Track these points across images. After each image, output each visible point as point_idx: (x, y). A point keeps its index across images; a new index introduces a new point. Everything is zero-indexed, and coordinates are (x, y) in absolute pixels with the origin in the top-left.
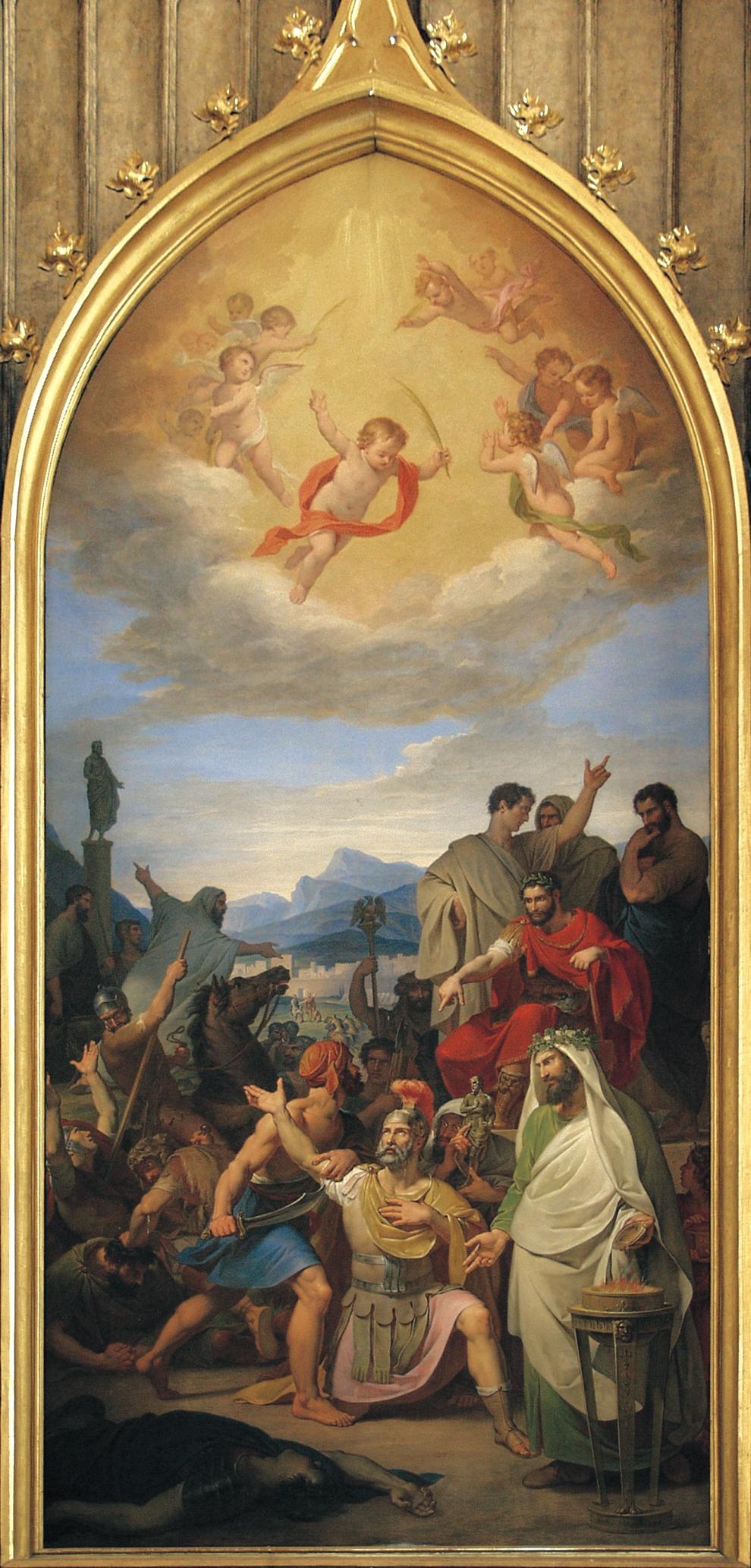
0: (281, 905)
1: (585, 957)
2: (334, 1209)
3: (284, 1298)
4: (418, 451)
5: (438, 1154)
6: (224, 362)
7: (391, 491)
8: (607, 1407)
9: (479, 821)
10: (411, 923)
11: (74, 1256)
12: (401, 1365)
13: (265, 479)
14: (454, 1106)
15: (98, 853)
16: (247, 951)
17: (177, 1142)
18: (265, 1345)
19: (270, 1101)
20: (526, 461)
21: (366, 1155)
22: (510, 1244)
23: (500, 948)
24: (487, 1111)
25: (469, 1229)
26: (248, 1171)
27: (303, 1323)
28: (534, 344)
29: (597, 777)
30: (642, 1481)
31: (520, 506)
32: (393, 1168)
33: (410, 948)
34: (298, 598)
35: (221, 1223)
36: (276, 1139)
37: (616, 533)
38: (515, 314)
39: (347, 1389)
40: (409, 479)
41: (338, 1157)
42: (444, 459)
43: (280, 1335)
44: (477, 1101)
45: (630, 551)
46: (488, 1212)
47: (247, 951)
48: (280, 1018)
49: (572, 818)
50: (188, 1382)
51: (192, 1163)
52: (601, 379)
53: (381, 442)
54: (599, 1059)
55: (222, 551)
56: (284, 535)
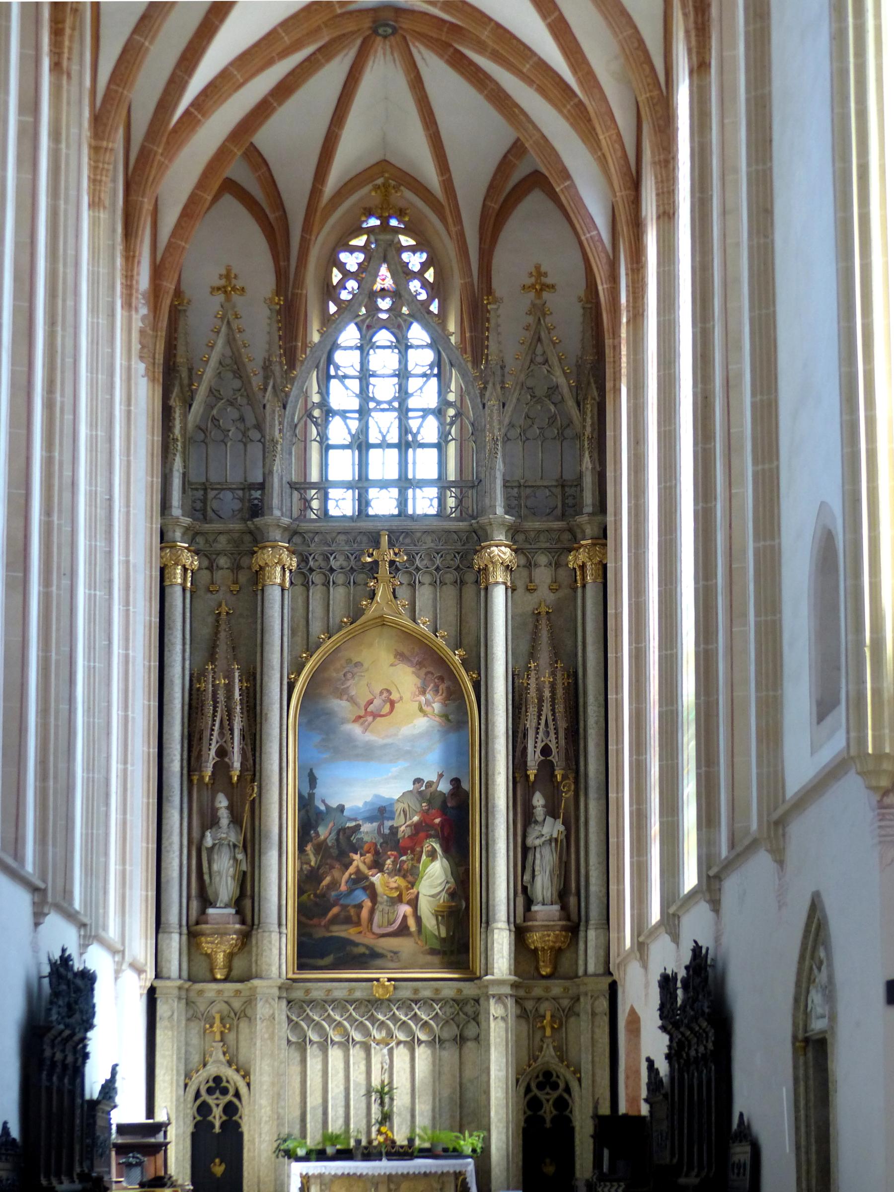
1: (437, 821)
2: (372, 885)
3: (360, 907)
4: (395, 696)
5: (400, 870)
6: (345, 675)
7: (388, 706)
8: (443, 934)
9: (410, 787)
10: (393, 813)
11: (305, 897)
12: (390, 923)
14: (404, 858)
15: (312, 796)
16: (350, 820)
19: (356, 857)
20: (423, 699)
21: (381, 870)
22: (418, 893)
23: (416, 819)
24: (412, 859)
25: (408, 889)
26: (350, 875)
27: (365, 913)
31: (421, 709)
32: (388, 874)
33: (393, 819)
34: (364, 732)
35: (343, 887)
36: (358, 867)
39: (376, 929)
40: (392, 704)
41: (374, 871)
42: (401, 698)
43: (359, 915)
44: (410, 857)
46: (413, 885)
47: (350, 820)
48: (359, 836)
49: (434, 786)
51: (336, 873)
53: (385, 694)
54: (441, 846)
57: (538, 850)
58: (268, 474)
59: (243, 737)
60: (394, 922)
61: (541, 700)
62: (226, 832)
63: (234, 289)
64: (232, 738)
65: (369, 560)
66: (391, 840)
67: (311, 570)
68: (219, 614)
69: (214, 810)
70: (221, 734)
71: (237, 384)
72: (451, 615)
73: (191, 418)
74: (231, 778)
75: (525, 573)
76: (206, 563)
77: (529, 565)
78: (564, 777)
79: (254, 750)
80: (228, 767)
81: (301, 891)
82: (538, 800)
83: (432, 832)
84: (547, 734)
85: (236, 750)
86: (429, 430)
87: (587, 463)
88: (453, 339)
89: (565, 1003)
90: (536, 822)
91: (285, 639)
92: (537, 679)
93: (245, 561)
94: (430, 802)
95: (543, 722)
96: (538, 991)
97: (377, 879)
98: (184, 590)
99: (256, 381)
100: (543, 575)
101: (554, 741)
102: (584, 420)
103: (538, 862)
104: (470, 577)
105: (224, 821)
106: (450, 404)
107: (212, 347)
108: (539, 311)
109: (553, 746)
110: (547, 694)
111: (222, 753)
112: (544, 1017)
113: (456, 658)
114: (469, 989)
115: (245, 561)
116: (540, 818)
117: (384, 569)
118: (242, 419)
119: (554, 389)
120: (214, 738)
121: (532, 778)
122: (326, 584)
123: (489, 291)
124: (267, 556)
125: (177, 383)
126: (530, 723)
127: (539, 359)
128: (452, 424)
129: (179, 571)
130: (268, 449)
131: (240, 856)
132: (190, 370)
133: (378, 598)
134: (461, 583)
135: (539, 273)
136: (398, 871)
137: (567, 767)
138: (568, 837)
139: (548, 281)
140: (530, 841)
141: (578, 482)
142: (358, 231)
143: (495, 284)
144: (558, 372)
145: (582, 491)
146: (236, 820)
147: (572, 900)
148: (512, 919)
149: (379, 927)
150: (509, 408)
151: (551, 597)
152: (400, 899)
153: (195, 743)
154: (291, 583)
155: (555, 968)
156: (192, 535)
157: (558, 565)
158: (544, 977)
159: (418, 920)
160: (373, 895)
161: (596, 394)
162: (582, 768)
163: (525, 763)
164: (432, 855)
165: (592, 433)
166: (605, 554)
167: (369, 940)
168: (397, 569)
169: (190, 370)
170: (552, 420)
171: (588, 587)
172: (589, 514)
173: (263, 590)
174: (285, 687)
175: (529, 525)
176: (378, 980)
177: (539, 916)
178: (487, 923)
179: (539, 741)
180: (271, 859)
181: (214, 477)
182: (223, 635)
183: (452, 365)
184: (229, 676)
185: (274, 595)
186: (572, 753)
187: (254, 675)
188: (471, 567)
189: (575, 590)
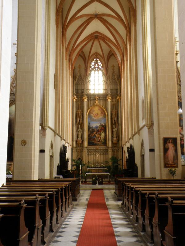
1: (103, 128)
3: (95, 138)
9: (100, 124)
19: (94, 133)
27: (95, 139)
35: (93, 136)
46: (100, 136)
58: (84, 88)
62: (80, 130)
66: (98, 131)
69: (79, 127)
72: (104, 105)
77: (113, 99)
81: (88, 137)
82: (114, 126)
87: (119, 87)
89: (117, 150)
94: (102, 126)
96: (114, 148)
97: (96, 135)
99: (83, 78)
100: (114, 100)
108: (113, 69)
110: (115, 114)
111: (79, 120)
113: (105, 110)
114: (107, 148)
117: (97, 99)
118: (81, 82)
119: (115, 78)
124: (84, 98)
130: (84, 85)
131: (81, 132)
134: (105, 101)
135: (113, 65)
136: (99, 134)
139: (115, 66)
140: (113, 131)
141: (118, 89)
142: (94, 60)
146: (81, 128)
147: (118, 138)
151: (115, 102)
152: (99, 138)
156: (76, 95)
159: (101, 140)
160: (96, 137)
164: (102, 132)
167: (96, 142)
170: (115, 82)
181: (78, 89)
184: (80, 111)
185: (85, 102)
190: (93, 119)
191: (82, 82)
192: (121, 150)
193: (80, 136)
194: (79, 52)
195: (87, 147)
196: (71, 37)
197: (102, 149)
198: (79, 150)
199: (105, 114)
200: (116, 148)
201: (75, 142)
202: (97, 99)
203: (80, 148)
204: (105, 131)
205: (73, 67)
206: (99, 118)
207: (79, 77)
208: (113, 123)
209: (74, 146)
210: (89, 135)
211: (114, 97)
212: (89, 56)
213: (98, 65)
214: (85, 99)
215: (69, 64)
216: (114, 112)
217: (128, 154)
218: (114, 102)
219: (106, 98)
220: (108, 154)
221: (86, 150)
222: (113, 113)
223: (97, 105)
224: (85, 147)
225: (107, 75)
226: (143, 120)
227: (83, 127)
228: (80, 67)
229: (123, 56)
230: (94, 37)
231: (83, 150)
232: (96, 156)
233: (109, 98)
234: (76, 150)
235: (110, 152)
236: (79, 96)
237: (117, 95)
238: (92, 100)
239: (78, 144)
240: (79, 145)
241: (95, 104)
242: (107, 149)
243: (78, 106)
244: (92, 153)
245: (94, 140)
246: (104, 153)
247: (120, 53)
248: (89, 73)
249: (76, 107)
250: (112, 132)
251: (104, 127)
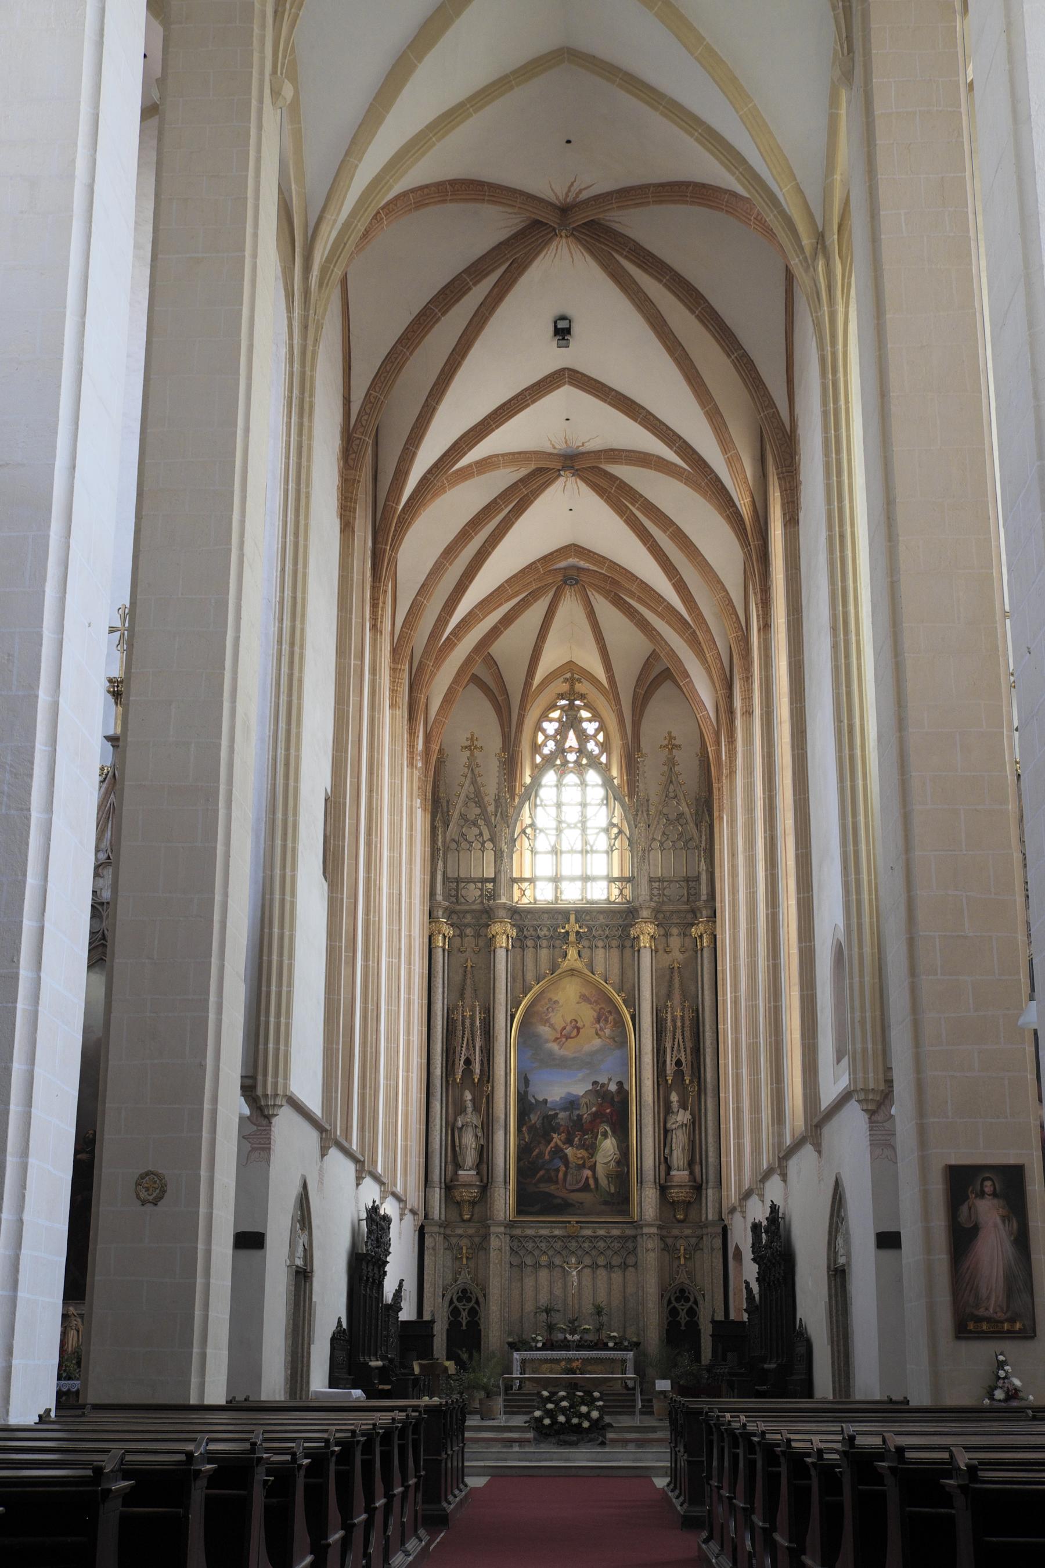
0: (557, 1102)
1: (608, 1111)
2: (566, 1155)
3: (557, 1170)
4: (580, 1024)
5: (584, 1145)
8: (612, 1190)
9: (591, 1087)
10: (579, 1105)
11: (521, 1163)
12: (578, 1182)
13: (554, 1029)
14: (586, 1137)
15: (526, 1092)
16: (551, 1109)
17: (540, 1143)
18: (554, 1178)
19: (555, 1136)
20: (598, 1026)
21: (572, 1145)
23: (594, 1109)
27: (561, 1175)
28: (599, 1006)
29: (610, 1080)
30: (618, 1203)
31: (597, 1034)
32: (577, 1148)
33: (579, 1109)
35: (547, 1157)
36: (556, 1142)
37: (613, 1038)
38: (596, 1002)
40: (578, 1029)
41: (567, 1145)
43: (557, 1176)
45: (615, 1042)
46: (592, 1155)
47: (551, 1109)
50: (542, 1185)
51: (542, 1147)
52: (610, 1012)
53: (574, 1023)
55: (547, 1041)
56: (557, 1038)
57: (674, 1132)
58: (497, 872)
59: (482, 1051)
60: (580, 1181)
61: (675, 1027)
62: (471, 1117)
63: (476, 748)
64: (475, 1053)
65: (563, 931)
66: (578, 1124)
67: (526, 937)
68: (467, 967)
69: (462, 1101)
70: (468, 1049)
71: (478, 811)
73: (448, 833)
74: (474, 1079)
75: (663, 939)
76: (458, 932)
78: (691, 1081)
79: (489, 1060)
80: (472, 1072)
81: (519, 1159)
82: (674, 1097)
83: (605, 1119)
84: (679, 1051)
85: (477, 1060)
86: (601, 842)
88: (616, 782)
89: (693, 1241)
90: (673, 1112)
91: (509, 984)
92: (672, 1014)
93: (483, 931)
94: (603, 1098)
95: (676, 1043)
96: (676, 1232)
97: (569, 1151)
98: (444, 950)
99: (491, 809)
100: (675, 942)
101: (684, 1056)
102: (701, 836)
103: (674, 1140)
104: (628, 943)
105: (470, 1110)
106: (614, 825)
107: (462, 786)
108: (671, 763)
109: (683, 1060)
110: (679, 1024)
111: (468, 1062)
112: (680, 1250)
114: (629, 1232)
115: (483, 931)
116: (675, 1110)
117: (572, 938)
118: (481, 834)
119: (681, 815)
120: (463, 1053)
121: (670, 1082)
122: (535, 947)
123: (639, 750)
124: (496, 928)
125: (440, 810)
126: (668, 1045)
127: (672, 795)
128: (616, 838)
129: (440, 938)
131: (479, 1134)
132: (448, 802)
133: (569, 957)
135: (671, 738)
136: (583, 1146)
137: (693, 1074)
138: (694, 1123)
139: (677, 742)
140: (669, 1126)
141: (698, 879)
143: (642, 745)
144: (684, 804)
145: (700, 884)
146: (476, 1109)
147: (697, 1168)
148: (657, 1181)
149: (570, 1185)
150: (652, 828)
152: (583, 1166)
153: (451, 1055)
154: (513, 946)
155: (686, 1216)
156: (450, 913)
157: (685, 935)
158: (679, 1221)
159: (596, 1180)
161: (708, 819)
162: (702, 1075)
163: (665, 1070)
164: (605, 1135)
165: (706, 844)
166: (715, 928)
168: (581, 937)
169: (448, 802)
171: (705, 950)
172: (704, 901)
173: (494, 951)
174: (509, 1018)
175: (665, 908)
176: (569, 1222)
177: (675, 1179)
178: (641, 1183)
179: (674, 1056)
180: (499, 1136)
182: (468, 981)
183: (615, 799)
184: (473, 1010)
185: (501, 954)
186: (695, 1065)
187: (489, 1008)
188: (629, 935)
189: (696, 952)
190: (551, 1054)
191: (486, 835)
192: (718, 1243)
193: (470, 1157)
194: (469, 661)
195: (511, 1225)
196: (422, 579)
197: (602, 1232)
198: (465, 1243)
199: (620, 1023)
200: (688, 1232)
201: (437, 1190)
202: (572, 938)
203: (471, 1231)
204: (621, 1129)
205: (435, 747)
206: (587, 1048)
207: (466, 804)
208: (670, 1079)
209: (437, 1210)
210: (523, 1151)
211: (677, 925)
212: (528, 683)
213: (583, 737)
214: (503, 934)
215: (412, 733)
216: (676, 1011)
217: (755, 1268)
218: (676, 954)
219: (626, 927)
220: (635, 1266)
221: (505, 1243)
222: (669, 1023)
223: (572, 972)
224: (499, 1224)
225: (631, 795)
226: (839, 1061)
227: (490, 1098)
228: (471, 747)
229: (730, 686)
230: (560, 578)
231: (486, 1237)
232: (565, 1274)
233: (646, 933)
234: (446, 1237)
235: (650, 1254)
236: (469, 919)
237: (694, 912)
238: (544, 943)
239: (458, 1203)
240: (466, 1208)
241: (565, 965)
242: (635, 1237)
243: (458, 978)
244: (544, 1259)
245: (556, 1182)
246: (616, 1261)
247: (708, 670)
248: (528, 780)
249: (449, 984)
250: (665, 1134)
251: (612, 1103)
